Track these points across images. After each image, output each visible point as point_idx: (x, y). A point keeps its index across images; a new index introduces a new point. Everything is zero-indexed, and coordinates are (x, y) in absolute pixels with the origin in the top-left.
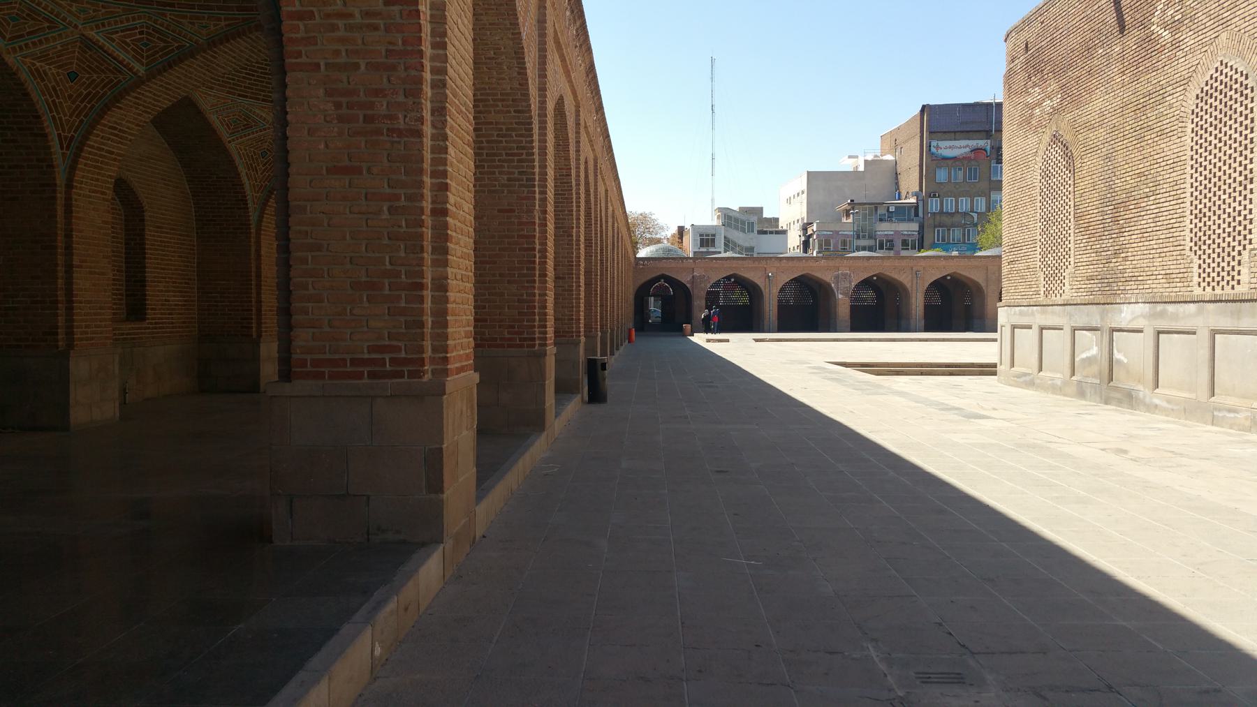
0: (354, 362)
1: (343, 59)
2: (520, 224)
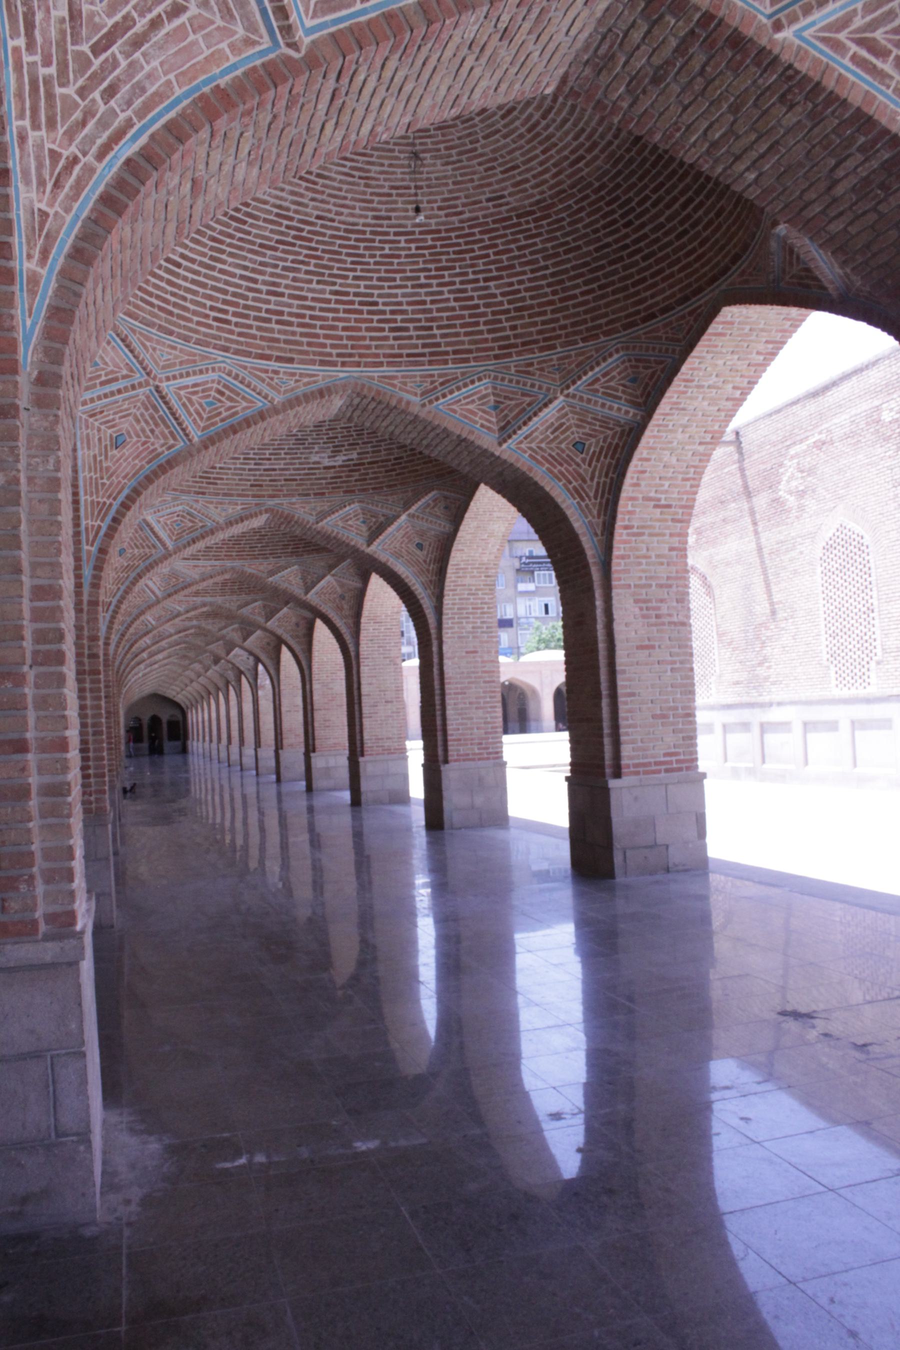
0: (656, 763)
1: (643, 582)
2: (483, 662)
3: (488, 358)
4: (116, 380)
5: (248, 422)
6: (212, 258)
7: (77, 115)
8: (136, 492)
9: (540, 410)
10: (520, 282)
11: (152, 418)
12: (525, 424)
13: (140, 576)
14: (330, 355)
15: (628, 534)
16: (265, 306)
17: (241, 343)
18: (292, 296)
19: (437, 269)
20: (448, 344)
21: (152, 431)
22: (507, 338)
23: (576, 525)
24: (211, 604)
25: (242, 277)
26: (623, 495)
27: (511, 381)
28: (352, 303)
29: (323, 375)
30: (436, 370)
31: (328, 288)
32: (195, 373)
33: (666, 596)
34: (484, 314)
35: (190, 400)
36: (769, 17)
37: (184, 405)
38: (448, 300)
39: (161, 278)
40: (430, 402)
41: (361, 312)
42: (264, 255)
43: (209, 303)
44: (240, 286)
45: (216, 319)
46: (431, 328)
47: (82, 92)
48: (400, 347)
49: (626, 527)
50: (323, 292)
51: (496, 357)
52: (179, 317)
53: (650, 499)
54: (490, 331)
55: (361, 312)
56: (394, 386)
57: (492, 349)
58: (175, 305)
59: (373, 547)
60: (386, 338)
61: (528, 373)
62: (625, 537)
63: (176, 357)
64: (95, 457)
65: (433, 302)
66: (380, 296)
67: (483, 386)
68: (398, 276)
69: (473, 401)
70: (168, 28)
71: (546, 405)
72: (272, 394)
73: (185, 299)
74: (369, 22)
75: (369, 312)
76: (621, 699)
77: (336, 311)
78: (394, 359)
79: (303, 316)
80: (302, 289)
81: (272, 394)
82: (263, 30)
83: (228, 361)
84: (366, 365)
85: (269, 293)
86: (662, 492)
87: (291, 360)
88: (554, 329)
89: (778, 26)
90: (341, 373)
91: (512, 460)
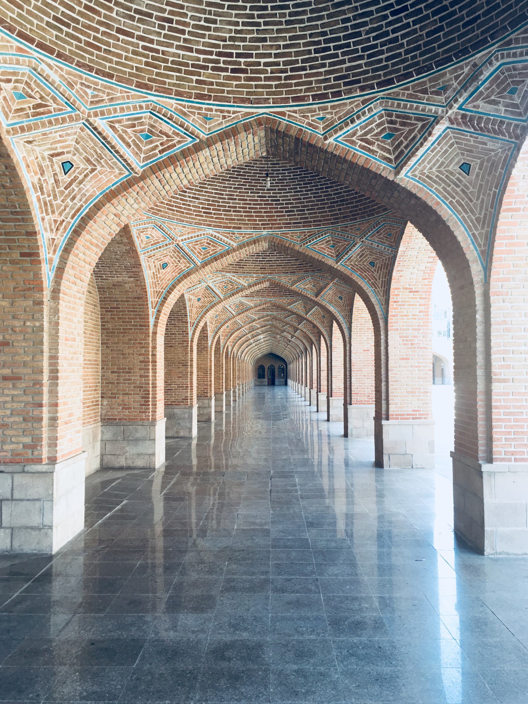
0: (407, 415)
1: (405, 327)
3: (328, 224)
4: (159, 243)
5: (222, 256)
6: (200, 187)
7: (63, 208)
8: (174, 286)
9: (352, 248)
10: (341, 189)
11: (178, 256)
12: (346, 254)
13: (208, 311)
14: (258, 225)
15: (396, 305)
16: (228, 205)
17: (217, 222)
18: (239, 200)
19: (304, 184)
20: (311, 218)
21: (179, 261)
22: (337, 214)
24: (271, 315)
25: (216, 193)
26: (392, 287)
27: (338, 235)
28: (268, 200)
29: (255, 234)
30: (306, 230)
31: (256, 195)
32: (195, 237)
33: (417, 334)
35: (194, 248)
36: (323, 135)
37: (192, 250)
38: (311, 197)
39: (177, 198)
40: (304, 244)
41: (272, 204)
42: (225, 184)
43: (201, 206)
44: (216, 197)
45: (204, 213)
46: (304, 210)
47: (63, 201)
48: (290, 219)
49: (395, 302)
50: (254, 196)
51: (332, 223)
52: (186, 213)
53: (406, 289)
54: (330, 211)
55: (272, 204)
56: (288, 237)
57: (330, 220)
58: (185, 209)
59: (319, 298)
60: (284, 216)
61: (345, 231)
62: (395, 306)
63: (186, 231)
64: (154, 273)
65: (304, 198)
66: (280, 197)
67: (327, 237)
68: (287, 188)
69: (323, 244)
70: (91, 176)
71: (354, 246)
72: (232, 243)
73: (189, 206)
74: (163, 161)
75: (276, 204)
76: (390, 383)
77: (261, 204)
79: (246, 208)
80: (244, 196)
81: (232, 243)
82: (125, 170)
84: (275, 228)
85: (229, 199)
86: (413, 285)
87: (240, 228)
88: (356, 211)
89: (326, 139)
90: (265, 232)
91: (342, 270)
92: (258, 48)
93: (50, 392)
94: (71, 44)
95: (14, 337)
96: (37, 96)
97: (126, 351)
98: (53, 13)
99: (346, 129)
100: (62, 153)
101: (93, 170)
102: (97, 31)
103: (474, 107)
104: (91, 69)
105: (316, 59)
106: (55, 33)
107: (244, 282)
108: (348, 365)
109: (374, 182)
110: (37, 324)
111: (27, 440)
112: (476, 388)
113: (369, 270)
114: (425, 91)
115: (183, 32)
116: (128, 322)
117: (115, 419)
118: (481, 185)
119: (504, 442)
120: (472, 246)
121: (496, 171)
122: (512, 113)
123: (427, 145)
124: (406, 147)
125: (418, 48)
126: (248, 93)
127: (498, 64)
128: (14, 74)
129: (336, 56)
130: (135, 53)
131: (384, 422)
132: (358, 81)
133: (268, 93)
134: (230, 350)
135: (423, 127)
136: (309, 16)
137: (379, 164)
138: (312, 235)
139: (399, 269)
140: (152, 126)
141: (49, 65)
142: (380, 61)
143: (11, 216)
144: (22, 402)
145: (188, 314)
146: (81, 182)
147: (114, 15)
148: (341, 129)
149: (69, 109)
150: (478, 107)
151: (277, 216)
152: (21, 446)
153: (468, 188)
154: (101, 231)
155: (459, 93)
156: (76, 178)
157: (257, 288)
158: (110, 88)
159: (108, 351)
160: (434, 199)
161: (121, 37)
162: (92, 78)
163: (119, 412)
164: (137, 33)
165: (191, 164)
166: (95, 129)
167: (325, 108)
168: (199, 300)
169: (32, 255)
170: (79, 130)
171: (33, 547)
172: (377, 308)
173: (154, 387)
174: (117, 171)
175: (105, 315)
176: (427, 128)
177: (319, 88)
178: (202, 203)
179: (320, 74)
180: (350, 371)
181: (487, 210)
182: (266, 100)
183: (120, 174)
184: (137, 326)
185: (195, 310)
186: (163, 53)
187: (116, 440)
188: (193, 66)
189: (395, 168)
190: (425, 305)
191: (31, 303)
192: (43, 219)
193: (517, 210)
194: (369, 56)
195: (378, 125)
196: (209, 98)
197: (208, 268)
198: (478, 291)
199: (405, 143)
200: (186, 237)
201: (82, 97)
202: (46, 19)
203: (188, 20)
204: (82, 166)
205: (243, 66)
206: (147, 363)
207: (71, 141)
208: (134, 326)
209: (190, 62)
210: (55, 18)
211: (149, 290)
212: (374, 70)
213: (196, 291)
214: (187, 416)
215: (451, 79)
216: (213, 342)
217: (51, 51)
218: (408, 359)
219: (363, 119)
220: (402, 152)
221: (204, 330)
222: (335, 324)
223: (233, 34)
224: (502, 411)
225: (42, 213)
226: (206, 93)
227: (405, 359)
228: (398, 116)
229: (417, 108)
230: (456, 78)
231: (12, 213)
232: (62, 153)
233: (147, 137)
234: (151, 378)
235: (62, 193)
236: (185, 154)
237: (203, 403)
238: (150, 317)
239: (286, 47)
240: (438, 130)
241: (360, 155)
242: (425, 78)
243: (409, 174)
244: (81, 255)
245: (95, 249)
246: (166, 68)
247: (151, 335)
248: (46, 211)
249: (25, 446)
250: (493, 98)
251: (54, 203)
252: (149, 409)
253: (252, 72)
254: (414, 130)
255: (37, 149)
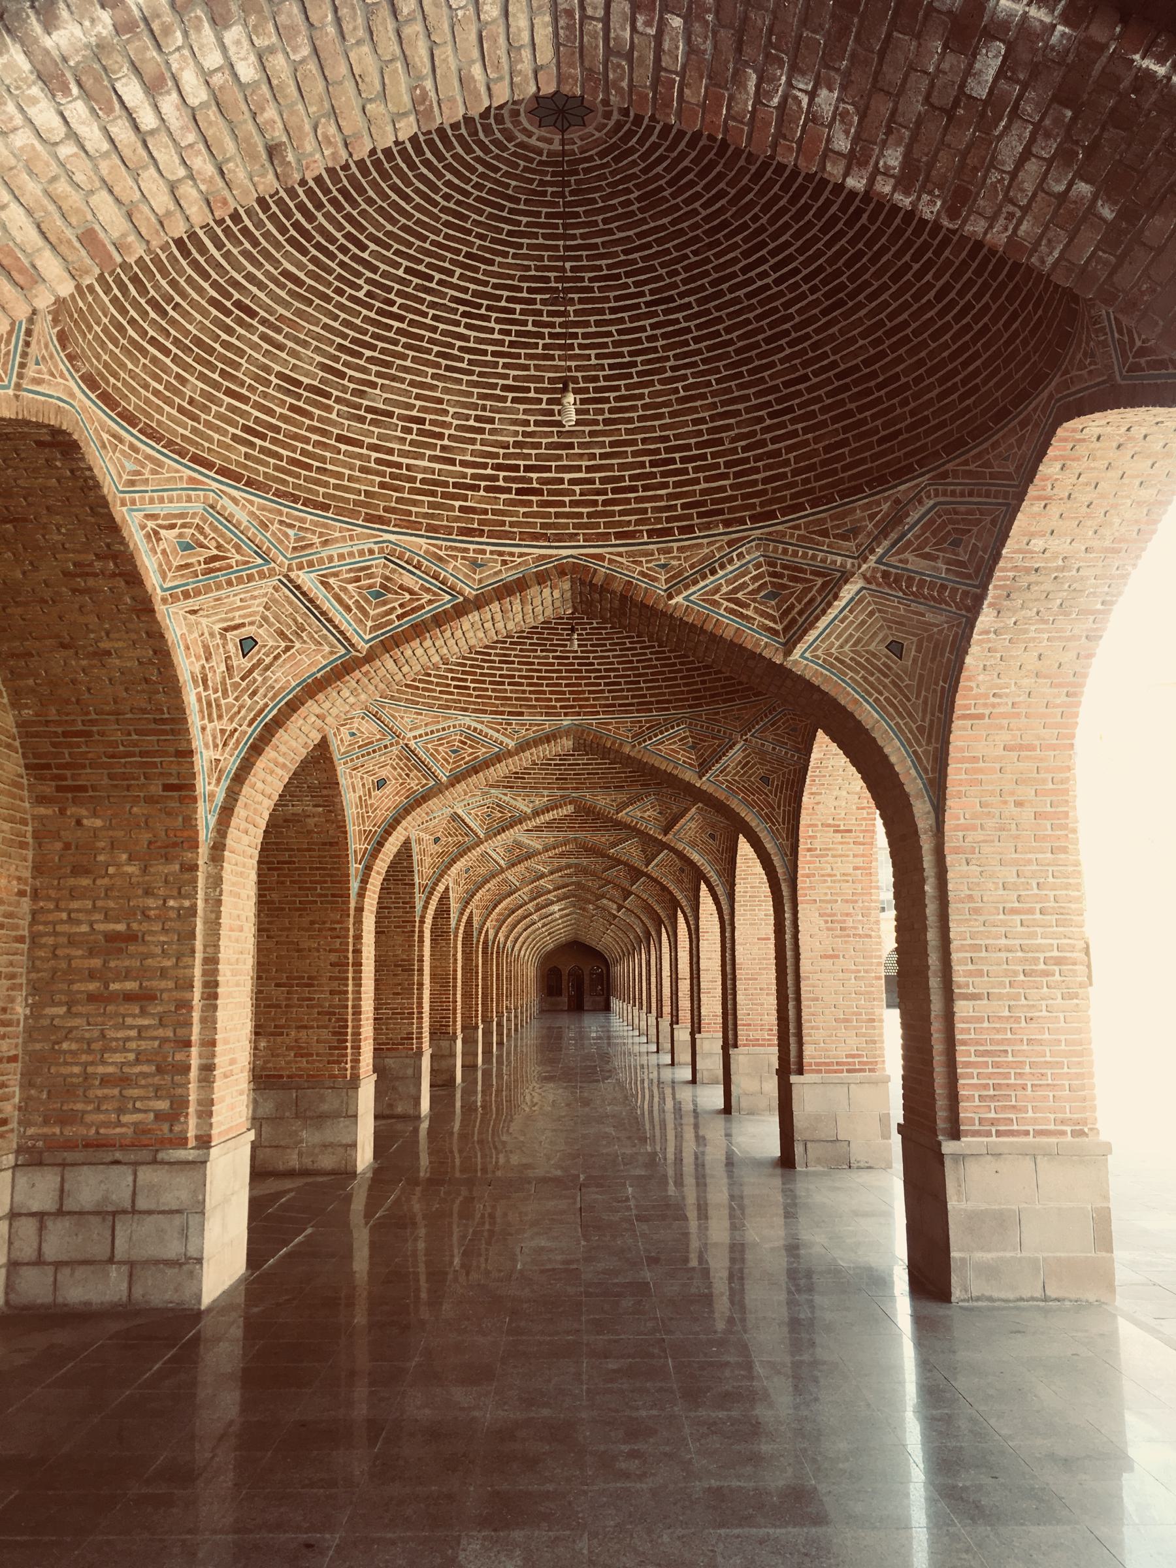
3: (683, 707)
5: (487, 764)
7: (236, 709)
13: (454, 861)
14: (555, 707)
20: (652, 696)
22: (699, 691)
23: (768, 846)
26: (802, 822)
29: (548, 724)
30: (643, 716)
34: (680, 671)
38: (650, 660)
45: (456, 687)
47: (236, 699)
48: (614, 698)
49: (809, 850)
50: (547, 657)
51: (690, 706)
52: (424, 689)
53: (829, 826)
54: (685, 685)
57: (687, 700)
59: (670, 836)
67: (681, 730)
71: (731, 748)
72: (506, 740)
76: (804, 1003)
77: (560, 671)
78: (608, 708)
79: (532, 677)
81: (506, 740)
83: (468, 720)
84: (585, 714)
85: (500, 662)
87: (521, 714)
89: (670, 597)
90: (566, 722)
91: (710, 790)
92: (560, 457)
93: (203, 1020)
94: (266, 464)
95: (145, 926)
96: (213, 544)
97: (305, 945)
98: (241, 421)
99: (702, 584)
100: (243, 625)
101: (288, 649)
102: (307, 441)
103: (901, 561)
104: (296, 499)
105: (653, 475)
106: (244, 449)
107: (523, 806)
108: (728, 968)
109: (751, 663)
110: (187, 903)
111: (163, 1105)
112: (929, 1010)
113: (759, 791)
114: (824, 533)
115: (440, 436)
116: (308, 889)
117: (281, 1076)
118: (921, 676)
119: (977, 1103)
120: (913, 771)
121: (942, 655)
122: (958, 574)
123: (832, 613)
124: (800, 613)
125: (812, 468)
126: (543, 526)
127: (931, 502)
128: (182, 515)
129: (685, 472)
130: (363, 469)
131: (794, 1079)
132: (721, 512)
133: (575, 526)
134: (491, 937)
135: (825, 585)
136: (641, 413)
137: (757, 636)
138: (654, 728)
139: (814, 790)
140: (388, 579)
141: (234, 500)
142: (754, 483)
143: (153, 726)
144: (155, 1038)
145: (416, 869)
146: (267, 668)
147: (334, 416)
148: (695, 582)
149: (260, 561)
150: (906, 562)
151: (590, 692)
152: (152, 1115)
153: (902, 681)
154: (294, 744)
155: (877, 540)
156: (260, 661)
157: (548, 817)
158: (325, 526)
159: (271, 944)
160: (848, 694)
161: (343, 447)
162: (298, 512)
163: (288, 1063)
164: (367, 440)
165: (448, 634)
166: (298, 587)
167: (669, 551)
168: (437, 840)
169: (182, 788)
170: (271, 590)
171: (167, 1297)
172: (777, 861)
173: (357, 1012)
174: (327, 649)
175: (266, 875)
176: (831, 589)
177: (658, 520)
178: (451, 671)
179: (660, 498)
180: (734, 979)
181: (933, 715)
182: (573, 537)
183: (332, 653)
184: (326, 896)
185: (428, 860)
186: (409, 467)
187: (281, 1118)
188: (455, 485)
189: (784, 644)
190: (863, 856)
191: (177, 867)
192: (203, 729)
193: (980, 717)
194: (737, 475)
195: (755, 579)
196: (481, 533)
197: (461, 787)
198: (927, 844)
199: (798, 607)
200: (421, 731)
201: (281, 542)
202: (232, 430)
203: (448, 419)
204: (271, 643)
205: (535, 485)
206: (343, 965)
207: (257, 607)
208: (320, 895)
209: (451, 480)
210: (246, 429)
211: (352, 829)
212: (745, 497)
213: (432, 824)
214: (410, 1072)
215: (863, 519)
216: (459, 921)
217: (237, 478)
218: (837, 957)
219: (730, 568)
220: (794, 621)
221: (445, 897)
222: (703, 886)
223: (520, 438)
224: (972, 1049)
225: (203, 718)
226: (476, 526)
227: (831, 957)
228: (784, 567)
229: (814, 557)
230: (872, 517)
231: (155, 721)
232: (243, 625)
233: (378, 595)
234: (350, 996)
235: (236, 686)
236: (440, 620)
237: (439, 1047)
238: (352, 879)
239: (603, 456)
240: (848, 591)
241: (726, 622)
242: (823, 513)
243: (807, 655)
244: (259, 785)
245: (279, 771)
246: (412, 491)
247: (352, 912)
248: (210, 715)
249: (159, 1116)
250: (927, 550)
251: (223, 702)
252: (346, 1055)
253: (551, 493)
254: (810, 589)
255: (204, 621)
